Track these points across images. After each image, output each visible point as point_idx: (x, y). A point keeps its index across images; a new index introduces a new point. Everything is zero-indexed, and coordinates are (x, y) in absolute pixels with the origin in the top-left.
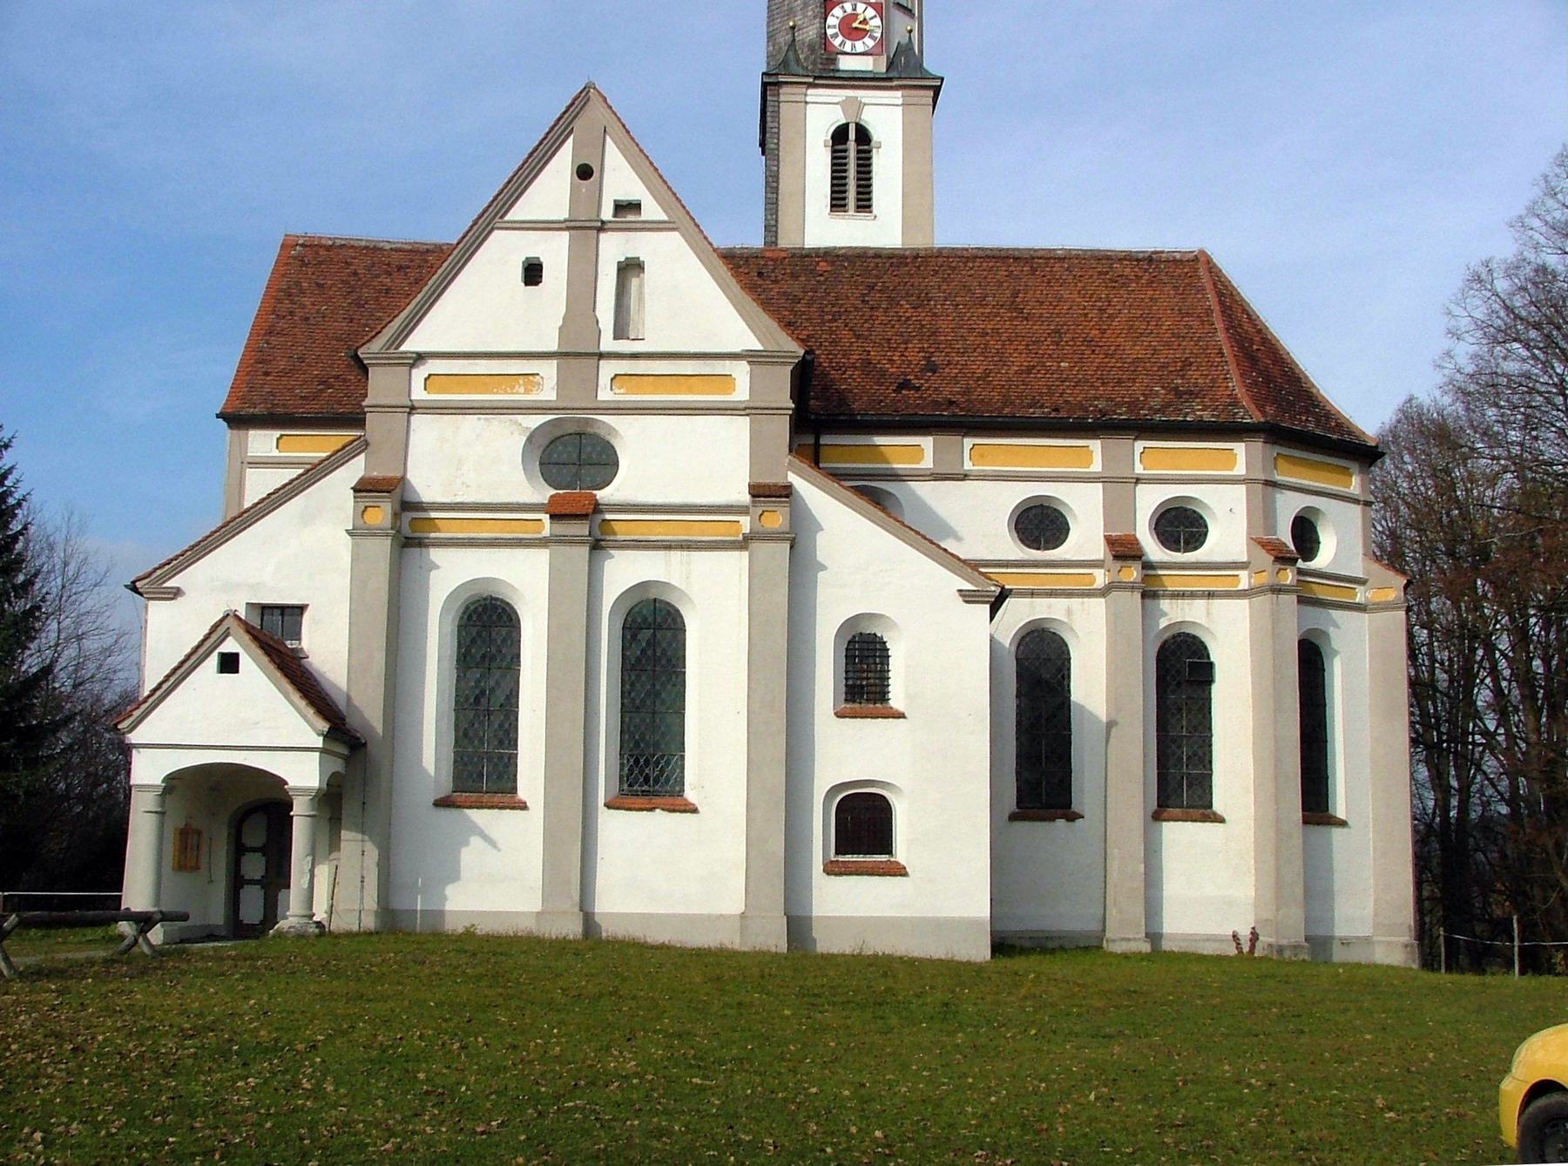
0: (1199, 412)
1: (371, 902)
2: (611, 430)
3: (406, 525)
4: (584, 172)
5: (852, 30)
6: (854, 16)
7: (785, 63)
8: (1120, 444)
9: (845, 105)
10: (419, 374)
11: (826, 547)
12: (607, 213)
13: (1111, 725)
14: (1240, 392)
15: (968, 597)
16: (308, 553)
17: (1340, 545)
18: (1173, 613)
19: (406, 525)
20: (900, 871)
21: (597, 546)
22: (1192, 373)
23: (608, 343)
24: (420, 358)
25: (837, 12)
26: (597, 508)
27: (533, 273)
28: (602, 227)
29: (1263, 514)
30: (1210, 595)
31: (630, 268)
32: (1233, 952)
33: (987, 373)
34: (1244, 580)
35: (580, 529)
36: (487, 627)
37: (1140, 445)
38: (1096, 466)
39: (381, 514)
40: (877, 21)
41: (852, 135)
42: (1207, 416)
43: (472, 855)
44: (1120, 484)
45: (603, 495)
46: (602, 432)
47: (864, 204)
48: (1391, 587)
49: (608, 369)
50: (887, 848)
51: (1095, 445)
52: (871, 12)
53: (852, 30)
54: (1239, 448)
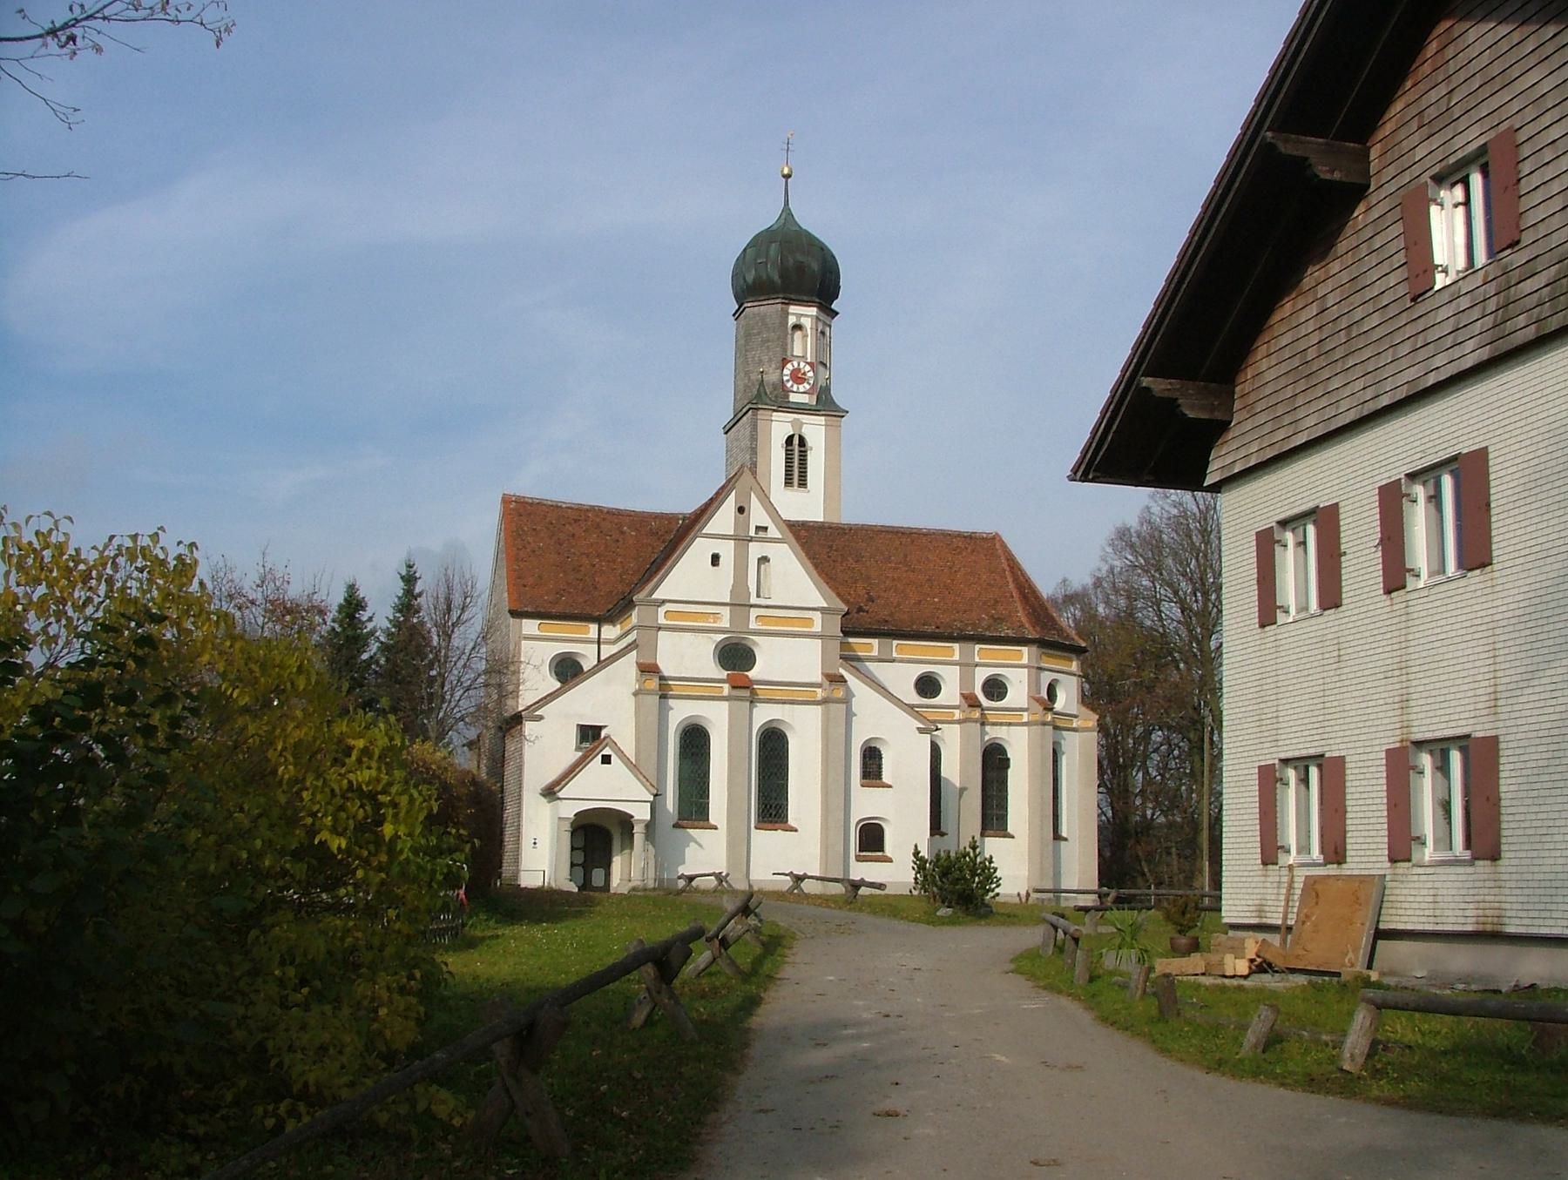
0: (1007, 632)
1: (651, 874)
2: (755, 643)
3: (657, 685)
4: (741, 510)
5: (798, 377)
6: (798, 370)
7: (759, 396)
8: (968, 646)
9: (794, 423)
10: (662, 610)
11: (856, 705)
12: (752, 533)
13: (962, 790)
14: (1024, 620)
15: (921, 731)
16: (610, 698)
17: (1067, 698)
18: (993, 733)
19: (657, 685)
20: (890, 861)
21: (753, 701)
22: (1000, 607)
23: (754, 600)
24: (664, 602)
25: (789, 366)
26: (752, 682)
27: (715, 560)
28: (751, 540)
29: (1034, 683)
30: (1010, 724)
31: (764, 560)
32: (1017, 900)
33: (899, 604)
34: (1025, 717)
35: (747, 693)
36: (695, 740)
37: (977, 647)
38: (957, 657)
39: (653, 684)
40: (811, 374)
41: (796, 441)
42: (1010, 633)
43: (691, 851)
44: (967, 666)
45: (752, 674)
46: (749, 644)
47: (803, 483)
48: (1091, 719)
49: (754, 612)
50: (881, 848)
51: (956, 646)
52: (808, 368)
53: (798, 377)
54: (1025, 649)
